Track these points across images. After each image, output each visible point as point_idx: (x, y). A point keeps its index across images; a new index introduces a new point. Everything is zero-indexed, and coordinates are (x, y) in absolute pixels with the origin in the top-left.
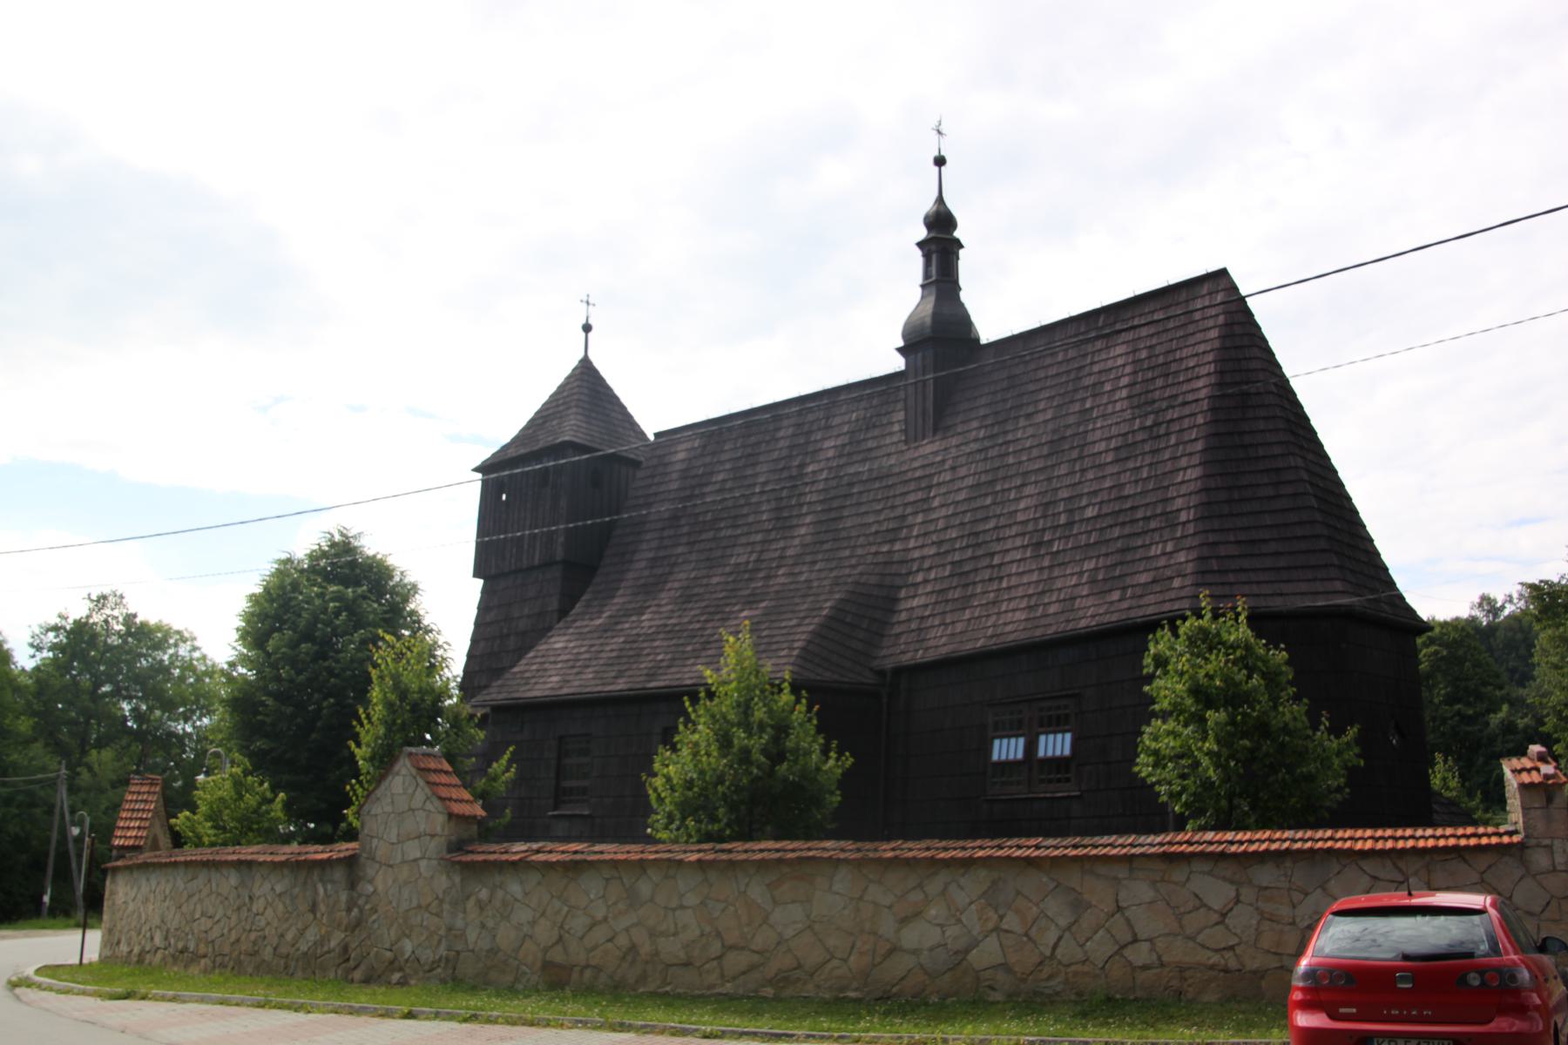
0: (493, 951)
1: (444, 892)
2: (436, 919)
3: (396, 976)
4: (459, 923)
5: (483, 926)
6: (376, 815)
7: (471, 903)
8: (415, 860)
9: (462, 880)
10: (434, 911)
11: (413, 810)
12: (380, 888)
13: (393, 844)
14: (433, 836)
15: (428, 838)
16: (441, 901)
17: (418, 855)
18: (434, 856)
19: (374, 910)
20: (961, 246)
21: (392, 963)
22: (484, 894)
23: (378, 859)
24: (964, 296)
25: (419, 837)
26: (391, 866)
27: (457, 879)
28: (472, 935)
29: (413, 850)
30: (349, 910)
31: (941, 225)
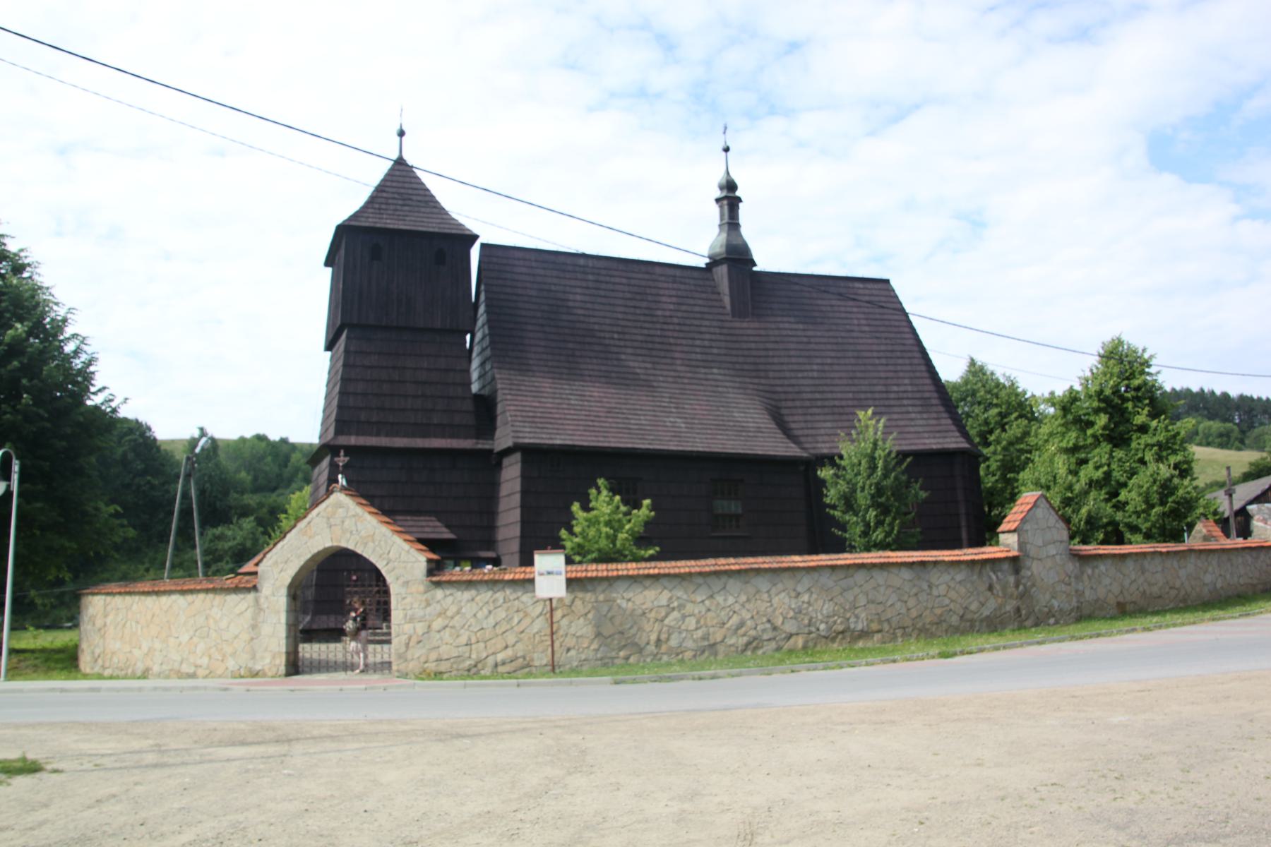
0: (1097, 600)
2: (1069, 587)
3: (1052, 621)
4: (1080, 588)
5: (1092, 588)
7: (1085, 577)
8: (1053, 556)
12: (1035, 572)
13: (1040, 547)
14: (1061, 542)
17: (1055, 553)
19: (1033, 585)
21: (1048, 614)
23: (1031, 555)
25: (1054, 543)
26: (1040, 560)
27: (1077, 565)
28: (1087, 593)
29: (1052, 550)
30: (1017, 586)
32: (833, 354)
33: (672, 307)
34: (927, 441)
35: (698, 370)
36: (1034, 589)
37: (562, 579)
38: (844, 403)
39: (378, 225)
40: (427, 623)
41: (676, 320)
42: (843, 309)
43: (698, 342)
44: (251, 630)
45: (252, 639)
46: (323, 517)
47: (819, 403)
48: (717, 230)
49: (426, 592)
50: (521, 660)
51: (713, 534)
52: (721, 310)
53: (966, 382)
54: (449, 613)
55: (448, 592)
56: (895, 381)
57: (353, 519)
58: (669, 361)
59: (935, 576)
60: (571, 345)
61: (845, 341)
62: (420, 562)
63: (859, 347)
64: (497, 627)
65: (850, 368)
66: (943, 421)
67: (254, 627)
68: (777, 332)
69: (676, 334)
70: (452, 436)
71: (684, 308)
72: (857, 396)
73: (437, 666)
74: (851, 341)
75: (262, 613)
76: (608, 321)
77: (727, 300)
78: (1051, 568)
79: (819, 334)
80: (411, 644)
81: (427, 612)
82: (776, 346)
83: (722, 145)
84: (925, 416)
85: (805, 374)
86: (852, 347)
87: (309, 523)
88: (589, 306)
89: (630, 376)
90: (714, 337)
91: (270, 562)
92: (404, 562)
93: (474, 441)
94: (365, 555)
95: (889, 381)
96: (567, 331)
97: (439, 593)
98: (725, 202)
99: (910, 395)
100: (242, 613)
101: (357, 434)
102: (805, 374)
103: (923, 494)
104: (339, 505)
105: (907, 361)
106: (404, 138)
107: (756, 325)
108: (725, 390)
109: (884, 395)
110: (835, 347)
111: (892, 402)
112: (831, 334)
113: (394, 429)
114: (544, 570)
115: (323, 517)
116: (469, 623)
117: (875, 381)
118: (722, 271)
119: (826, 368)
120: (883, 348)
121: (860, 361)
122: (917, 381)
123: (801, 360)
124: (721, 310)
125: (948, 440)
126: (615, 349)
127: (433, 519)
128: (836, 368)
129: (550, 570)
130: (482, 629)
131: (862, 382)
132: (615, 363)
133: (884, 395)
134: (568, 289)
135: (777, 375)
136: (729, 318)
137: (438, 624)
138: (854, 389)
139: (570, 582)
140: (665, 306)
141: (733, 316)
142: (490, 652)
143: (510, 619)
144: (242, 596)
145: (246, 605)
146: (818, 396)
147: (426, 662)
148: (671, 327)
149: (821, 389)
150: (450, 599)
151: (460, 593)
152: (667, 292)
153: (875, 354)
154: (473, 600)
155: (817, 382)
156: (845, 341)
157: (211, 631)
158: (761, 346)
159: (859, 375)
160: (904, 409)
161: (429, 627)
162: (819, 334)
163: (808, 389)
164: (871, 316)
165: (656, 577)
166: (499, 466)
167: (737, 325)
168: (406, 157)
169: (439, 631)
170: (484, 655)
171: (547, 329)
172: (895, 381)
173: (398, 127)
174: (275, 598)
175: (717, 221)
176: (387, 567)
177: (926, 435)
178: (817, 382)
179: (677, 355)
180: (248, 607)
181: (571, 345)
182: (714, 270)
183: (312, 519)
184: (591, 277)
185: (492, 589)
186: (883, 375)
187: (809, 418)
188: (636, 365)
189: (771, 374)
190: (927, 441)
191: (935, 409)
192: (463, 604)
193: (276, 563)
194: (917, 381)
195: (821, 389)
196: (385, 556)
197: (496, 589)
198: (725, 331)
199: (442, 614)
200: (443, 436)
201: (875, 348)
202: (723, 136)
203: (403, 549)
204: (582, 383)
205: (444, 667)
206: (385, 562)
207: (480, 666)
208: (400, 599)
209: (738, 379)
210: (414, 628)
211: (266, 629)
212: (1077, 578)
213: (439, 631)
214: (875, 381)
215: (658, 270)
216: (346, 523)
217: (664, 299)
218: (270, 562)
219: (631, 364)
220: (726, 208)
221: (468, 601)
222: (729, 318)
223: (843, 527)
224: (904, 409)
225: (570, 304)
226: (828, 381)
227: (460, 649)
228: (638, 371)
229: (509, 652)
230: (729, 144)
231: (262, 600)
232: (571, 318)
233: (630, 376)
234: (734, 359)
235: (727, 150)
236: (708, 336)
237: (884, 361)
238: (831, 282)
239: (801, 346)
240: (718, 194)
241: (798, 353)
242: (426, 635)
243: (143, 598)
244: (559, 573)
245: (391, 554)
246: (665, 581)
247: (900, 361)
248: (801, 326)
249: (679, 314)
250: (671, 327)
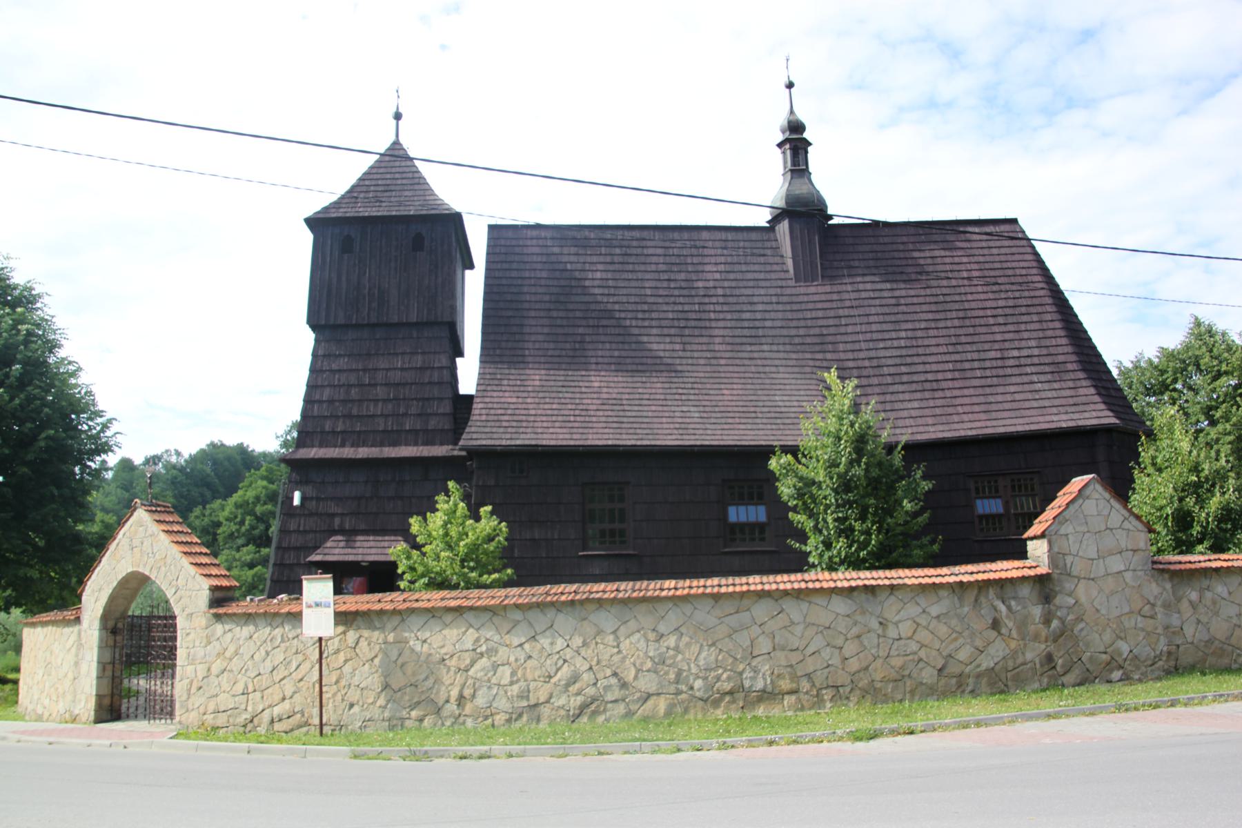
0: (1210, 642)
1: (1156, 597)
2: (1151, 621)
3: (1116, 675)
4: (1175, 620)
5: (1199, 622)
6: (1067, 535)
7: (1185, 605)
9: (1173, 587)
10: (1148, 614)
11: (1111, 529)
12: (1083, 599)
13: (1093, 560)
15: (1131, 553)
16: (1153, 605)
18: (1140, 568)
19: (1079, 619)
20: (810, 144)
21: (1108, 664)
22: (1194, 596)
23: (1074, 573)
24: (814, 178)
27: (1168, 586)
28: (1189, 630)
29: (1116, 564)
30: (1047, 621)
31: (796, 127)
32: (930, 316)
33: (717, 276)
34: (1055, 418)
35: (743, 348)
36: (1081, 625)
37: (330, 612)
38: (940, 376)
39: (348, 215)
41: (720, 292)
42: (948, 260)
43: (747, 315)
47: (905, 378)
50: (299, 716)
51: (726, 550)
52: (782, 275)
53: (1187, 348)
55: (227, 627)
56: (1017, 344)
58: (705, 340)
59: (890, 607)
60: (581, 330)
61: (948, 299)
63: (967, 305)
64: (274, 673)
65: (952, 331)
66: (1082, 391)
68: (853, 296)
69: (718, 308)
70: (426, 443)
71: (732, 276)
72: (959, 366)
73: (214, 718)
74: (957, 298)
76: (632, 299)
77: (790, 263)
78: (1113, 593)
79: (912, 292)
80: (192, 692)
82: (852, 312)
84: (1056, 385)
85: (889, 344)
86: (957, 306)
87: (118, 545)
88: (611, 283)
89: (649, 361)
90: (769, 307)
93: (450, 447)
95: (1007, 345)
96: (578, 314)
97: (219, 628)
98: (788, 146)
99: (1036, 360)
101: (321, 446)
102: (889, 344)
103: (926, 486)
105: (1035, 318)
106: (400, 122)
107: (828, 288)
108: (773, 369)
109: (1000, 363)
110: (933, 308)
111: (1009, 371)
112: (928, 292)
113: (360, 439)
114: (311, 602)
117: (986, 346)
118: (784, 227)
119: (919, 334)
120: (1001, 303)
121: (967, 322)
122: (1048, 342)
123: (885, 327)
124: (782, 275)
125: (1087, 415)
126: (636, 331)
127: (400, 538)
128: (931, 333)
129: (318, 600)
130: (260, 674)
131: (968, 348)
132: (634, 346)
133: (1000, 363)
134: (587, 267)
135: (849, 347)
136: (792, 283)
138: (957, 357)
140: (709, 276)
141: (797, 279)
146: (904, 369)
147: (205, 714)
148: (714, 300)
149: (909, 360)
150: (229, 635)
151: (239, 628)
152: (713, 260)
153: (989, 313)
154: (251, 637)
155: (904, 352)
156: (948, 299)
158: (832, 313)
159: (963, 339)
160: (1026, 379)
161: (209, 670)
162: (912, 292)
163: (890, 362)
164: (987, 266)
165: (459, 610)
167: (802, 290)
168: (401, 140)
171: (555, 314)
172: (1017, 344)
173: (394, 110)
175: (780, 169)
177: (1054, 410)
178: (904, 352)
179: (716, 332)
181: (581, 330)
182: (777, 228)
184: (618, 251)
186: (998, 337)
187: (888, 397)
188: (658, 346)
189: (841, 347)
190: (1055, 418)
191: (1072, 376)
194: (1048, 342)
195: (909, 360)
196: (175, 582)
197: (274, 624)
198: (785, 299)
200: (416, 444)
201: (989, 304)
204: (583, 373)
205: (222, 720)
206: (174, 591)
207: (256, 720)
209: (794, 356)
212: (1167, 606)
214: (986, 346)
215: (705, 235)
217: (708, 268)
219: (655, 347)
220: (788, 152)
221: (246, 639)
222: (792, 283)
223: (802, 537)
224: (1026, 379)
225: (587, 283)
226: (921, 351)
227: (237, 699)
228: (662, 354)
229: (286, 705)
232: (587, 299)
233: (649, 361)
234: (793, 332)
235: (790, 86)
236: (760, 307)
237: (1001, 320)
239: (886, 310)
241: (881, 318)
242: (205, 680)
246: (469, 616)
247: (1025, 318)
248: (888, 286)
249: (726, 284)
250: (714, 300)
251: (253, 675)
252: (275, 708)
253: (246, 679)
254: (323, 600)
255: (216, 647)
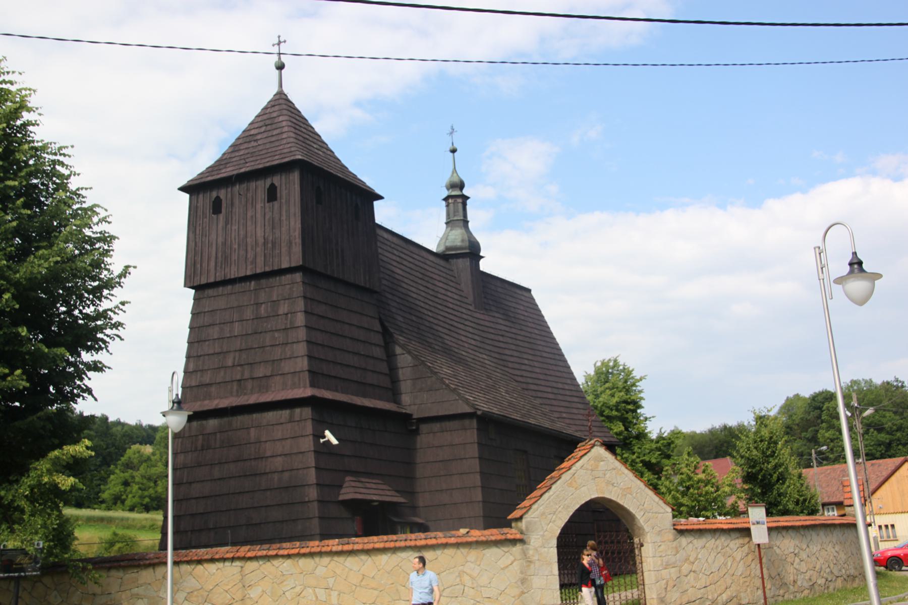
37: (765, 527)
40: (678, 568)
44: (519, 583)
45: (523, 593)
46: (587, 469)
48: (445, 226)
49: (675, 540)
50: (735, 599)
54: (692, 559)
57: (614, 472)
62: (667, 512)
67: (523, 581)
75: (532, 566)
80: (668, 589)
81: (677, 559)
83: (450, 147)
91: (537, 513)
92: (656, 513)
94: (626, 506)
97: (684, 540)
100: (507, 567)
104: (600, 459)
107: (487, 318)
114: (754, 521)
115: (587, 469)
116: (704, 569)
129: (758, 520)
130: (712, 573)
137: (686, 568)
139: (770, 529)
141: (475, 308)
142: (719, 592)
143: (725, 564)
144: (505, 549)
145: (512, 558)
150: (691, 545)
151: (696, 540)
154: (704, 547)
157: (466, 588)
165: (786, 528)
166: (416, 432)
168: (286, 90)
169: (686, 576)
170: (716, 595)
174: (546, 549)
176: (644, 517)
180: (515, 560)
183: (577, 470)
185: (714, 538)
192: (699, 551)
193: (543, 514)
196: (641, 507)
199: (687, 559)
202: (449, 138)
203: (654, 501)
208: (657, 547)
210: (670, 574)
211: (537, 582)
213: (686, 576)
216: (607, 476)
218: (537, 513)
227: (702, 590)
230: (456, 146)
231: (531, 552)
235: (454, 151)
238: (507, 286)
240: (446, 193)
243: (341, 559)
244: (763, 524)
245: (645, 506)
246: (790, 531)
251: (708, 574)
252: (723, 595)
253: (705, 576)
254: (761, 520)
255: (682, 554)
